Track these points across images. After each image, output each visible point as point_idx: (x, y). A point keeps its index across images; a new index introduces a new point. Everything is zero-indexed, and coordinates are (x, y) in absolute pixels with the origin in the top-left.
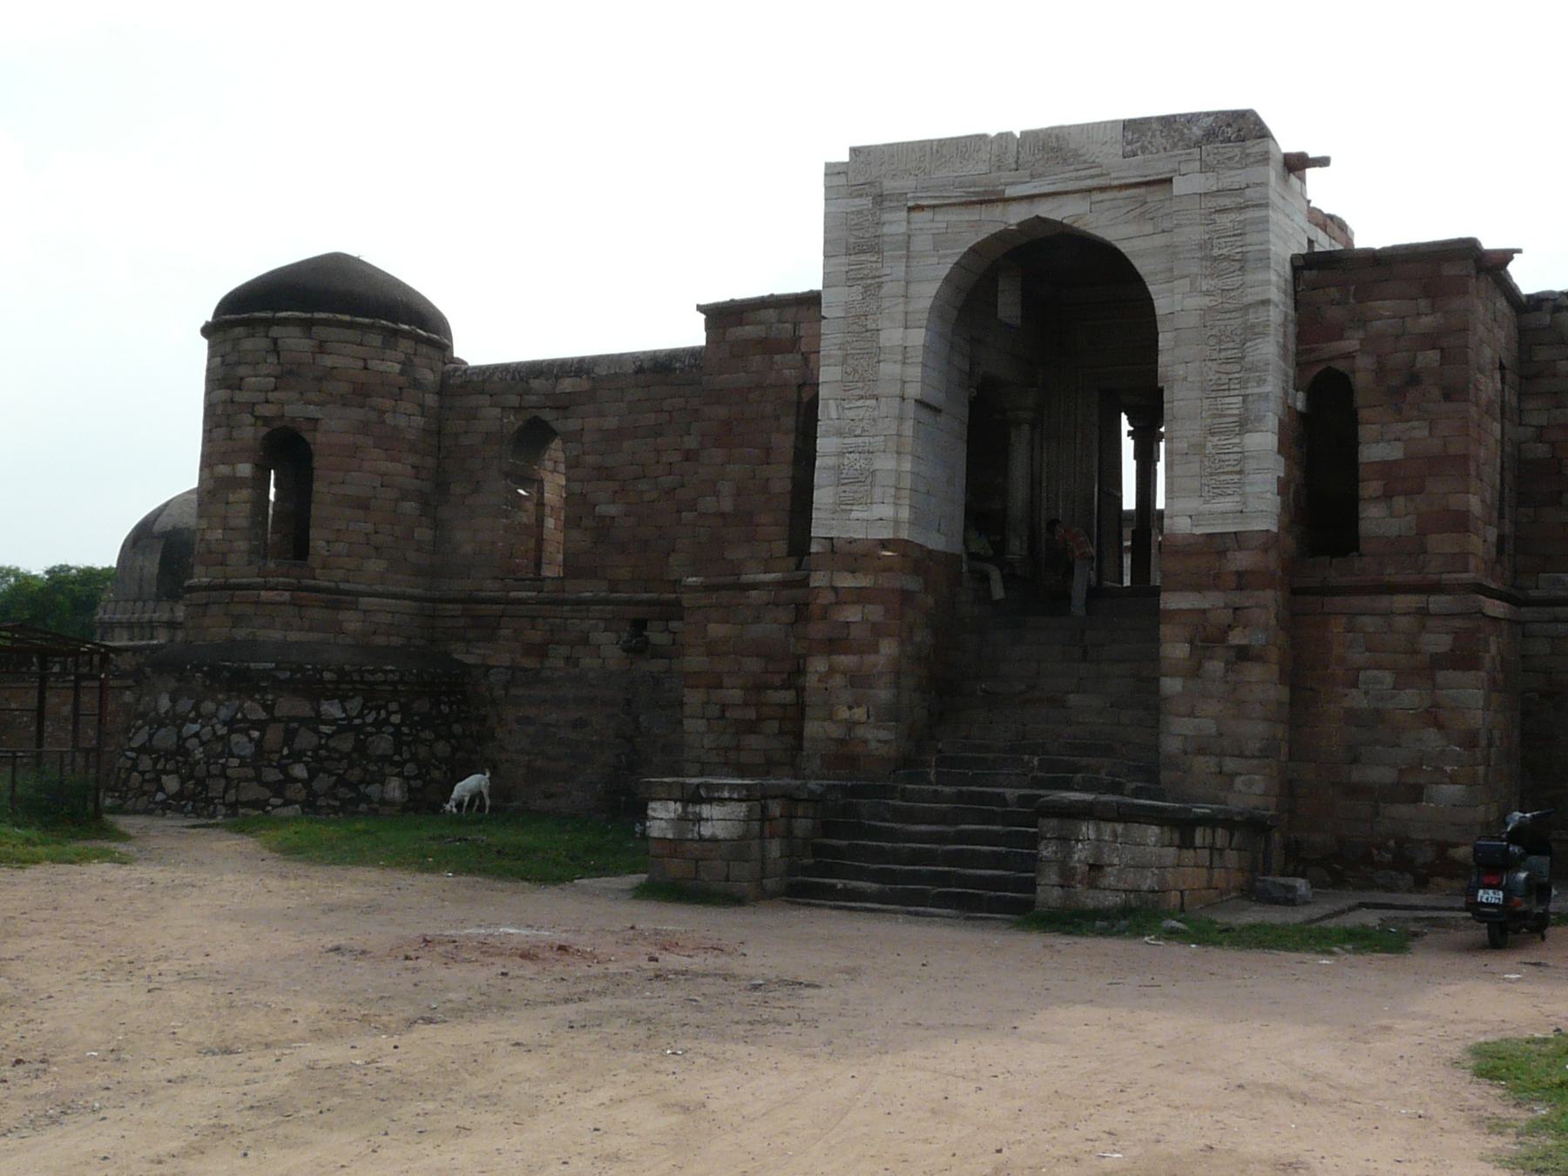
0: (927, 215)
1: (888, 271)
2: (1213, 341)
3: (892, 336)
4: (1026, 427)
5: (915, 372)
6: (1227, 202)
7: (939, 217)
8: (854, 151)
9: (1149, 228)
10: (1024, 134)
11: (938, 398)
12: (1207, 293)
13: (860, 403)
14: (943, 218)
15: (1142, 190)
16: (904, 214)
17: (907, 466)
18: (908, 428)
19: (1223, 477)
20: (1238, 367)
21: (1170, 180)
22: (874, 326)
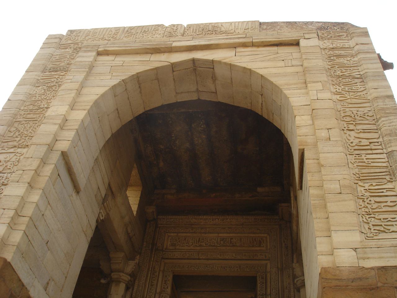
0: (110, 58)
1: (71, 77)
2: (348, 119)
3: (58, 108)
4: (122, 286)
5: (70, 135)
6: (342, 52)
7: (116, 59)
8: (71, 32)
9: (282, 64)
10: (189, 26)
11: (82, 180)
12: (337, 93)
13: (12, 150)
14: (119, 60)
15: (275, 49)
16: (94, 54)
17: (35, 197)
18: (48, 170)
19: (381, 217)
20: (376, 135)
21: (297, 44)
22: (46, 106)
